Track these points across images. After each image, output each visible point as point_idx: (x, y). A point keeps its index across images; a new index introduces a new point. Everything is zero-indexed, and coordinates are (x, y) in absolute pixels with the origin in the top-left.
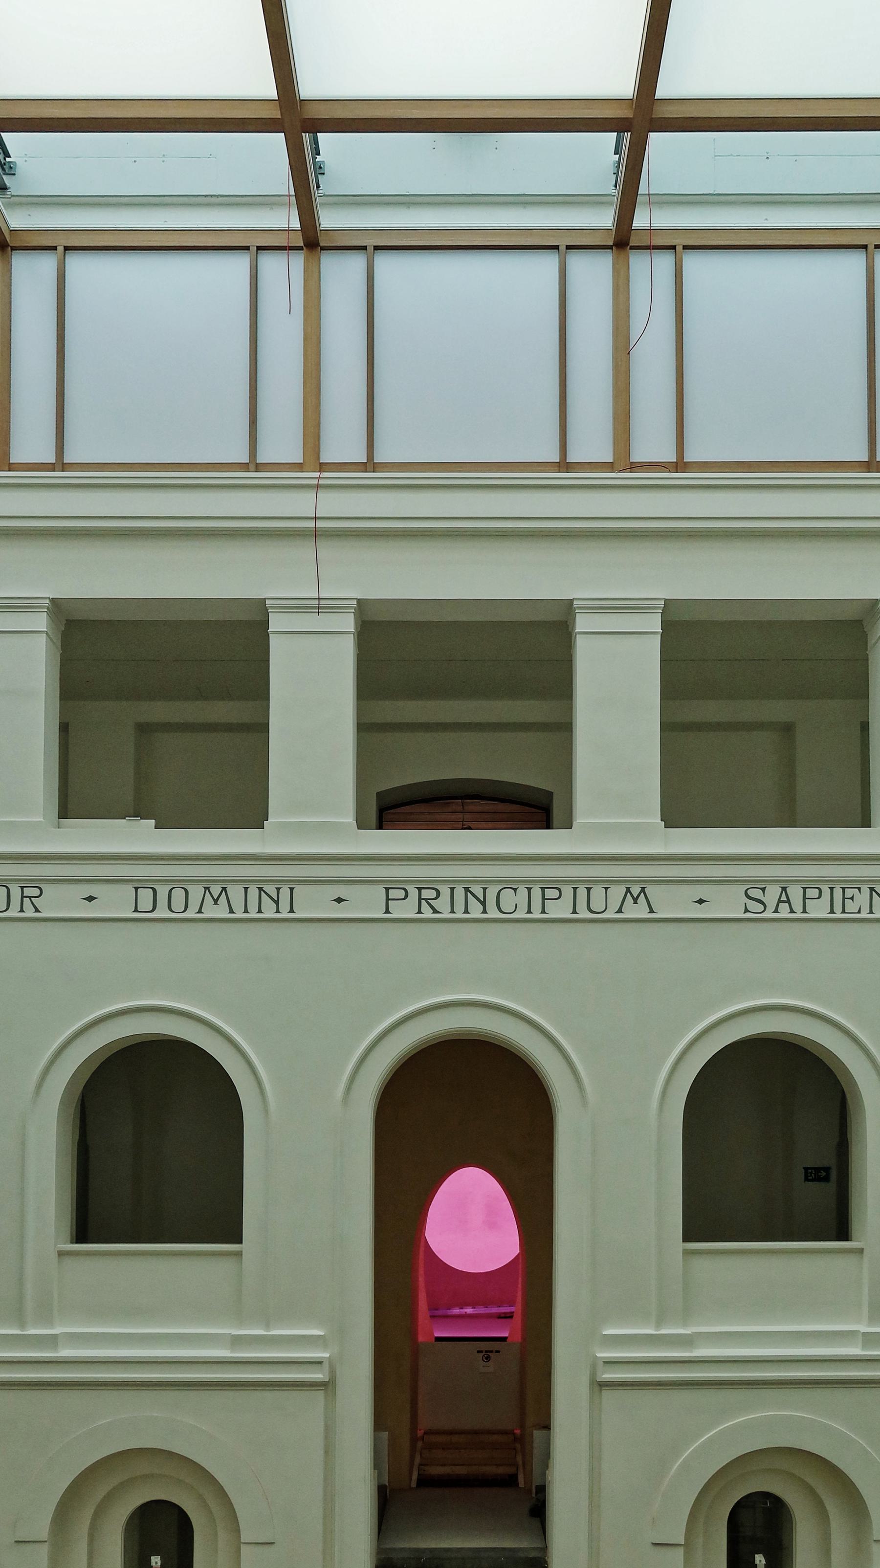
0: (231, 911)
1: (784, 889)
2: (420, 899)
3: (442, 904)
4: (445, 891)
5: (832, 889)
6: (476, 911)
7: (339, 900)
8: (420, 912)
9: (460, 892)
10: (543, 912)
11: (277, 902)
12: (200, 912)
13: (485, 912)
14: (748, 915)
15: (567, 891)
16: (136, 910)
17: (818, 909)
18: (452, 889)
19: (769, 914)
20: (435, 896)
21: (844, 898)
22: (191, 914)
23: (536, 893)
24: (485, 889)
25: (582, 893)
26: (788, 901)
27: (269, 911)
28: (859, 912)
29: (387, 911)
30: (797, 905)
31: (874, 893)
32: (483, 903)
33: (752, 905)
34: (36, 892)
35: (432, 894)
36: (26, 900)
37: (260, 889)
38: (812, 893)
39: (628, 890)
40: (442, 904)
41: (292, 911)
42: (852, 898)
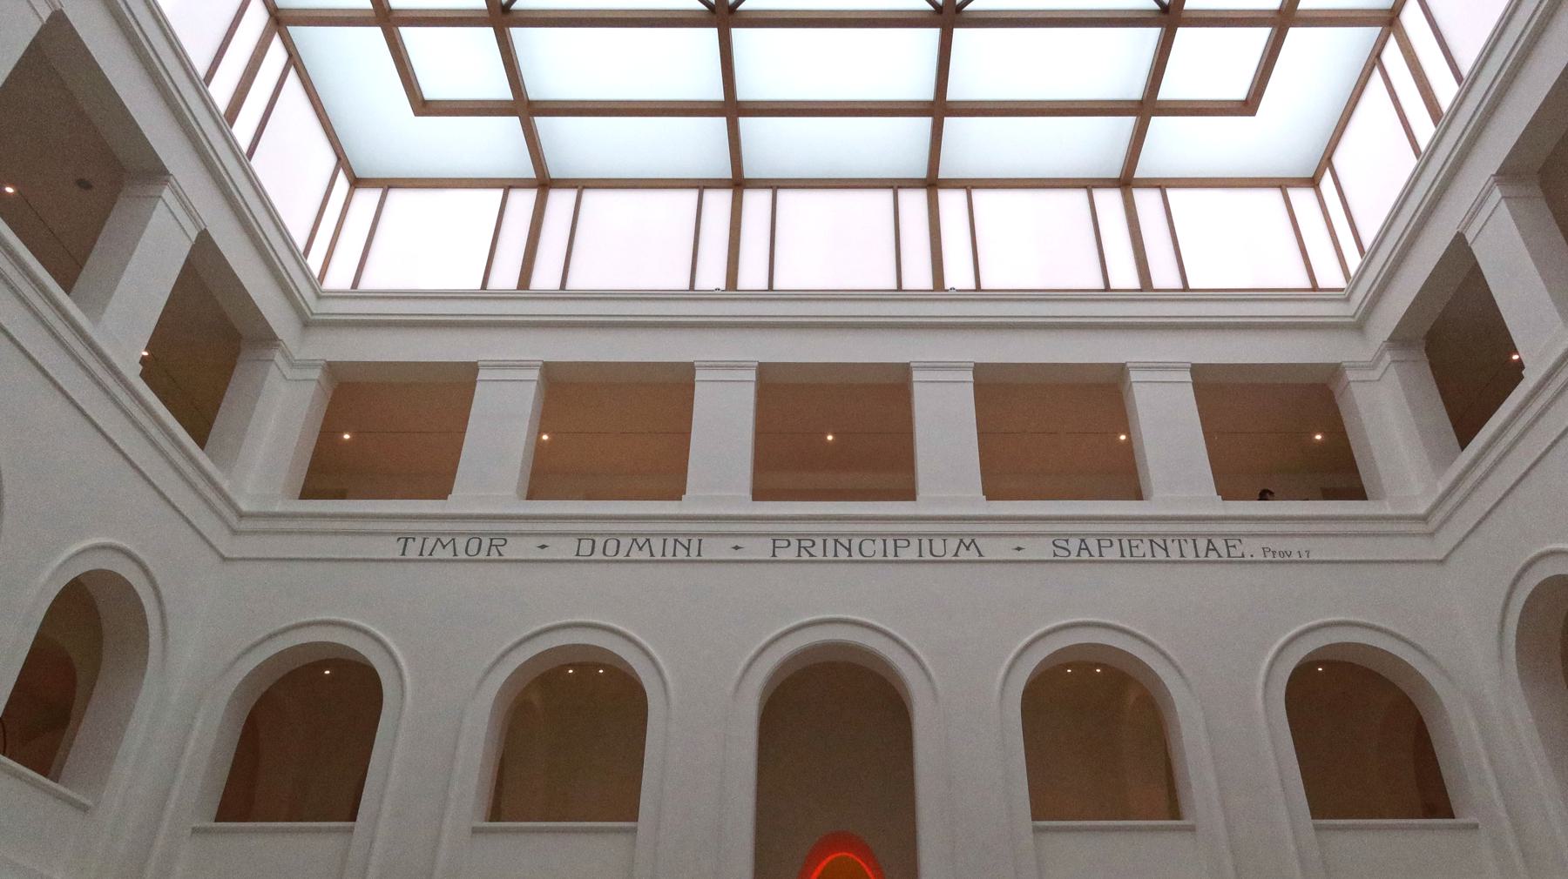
0: (652, 555)
1: (1083, 540)
2: (800, 547)
3: (818, 551)
4: (819, 542)
5: (1120, 540)
6: (843, 554)
7: (737, 548)
8: (799, 556)
9: (830, 543)
10: (896, 555)
11: (688, 549)
12: (628, 555)
13: (850, 555)
14: (1056, 558)
15: (914, 542)
17: (1112, 553)
18: (825, 541)
19: (1073, 557)
20: (811, 545)
21: (1131, 547)
22: (621, 556)
23: (890, 543)
24: (850, 541)
25: (925, 543)
26: (1087, 549)
27: (681, 554)
28: (1144, 556)
29: (774, 555)
30: (1095, 552)
31: (1154, 544)
32: (849, 550)
35: (809, 544)
36: (493, 548)
37: (676, 540)
38: (1105, 543)
39: (961, 541)
40: (818, 551)
41: (699, 555)
42: (1137, 547)
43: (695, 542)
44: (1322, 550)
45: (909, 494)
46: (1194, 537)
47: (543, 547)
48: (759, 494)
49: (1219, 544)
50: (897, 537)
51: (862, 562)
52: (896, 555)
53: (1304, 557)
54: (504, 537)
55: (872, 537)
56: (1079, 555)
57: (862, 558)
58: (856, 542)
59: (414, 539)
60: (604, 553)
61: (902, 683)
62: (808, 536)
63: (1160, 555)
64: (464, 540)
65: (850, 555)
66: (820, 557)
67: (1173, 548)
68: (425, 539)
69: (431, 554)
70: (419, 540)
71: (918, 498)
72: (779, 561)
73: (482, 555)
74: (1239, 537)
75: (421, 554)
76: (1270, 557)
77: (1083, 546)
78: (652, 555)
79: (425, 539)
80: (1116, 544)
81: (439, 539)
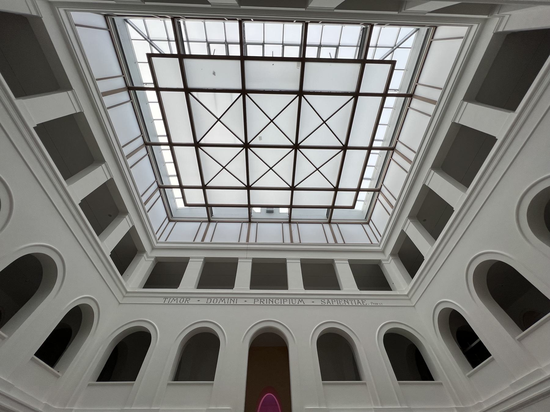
0: (225, 303)
1: (328, 300)
3: (265, 302)
4: (265, 300)
5: (337, 300)
7: (245, 301)
9: (268, 300)
10: (284, 303)
13: (273, 303)
15: (288, 300)
17: (335, 304)
19: (326, 304)
22: (217, 303)
23: (282, 300)
25: (291, 300)
29: (254, 303)
32: (273, 302)
33: (323, 303)
37: (231, 299)
39: (299, 300)
40: (265, 302)
41: (236, 303)
43: (235, 300)
44: (385, 303)
45: (286, 288)
46: (354, 299)
47: (199, 301)
48: (251, 288)
49: (360, 301)
50: (284, 299)
51: (275, 305)
52: (284, 303)
53: (381, 305)
54: (189, 298)
55: (278, 299)
56: (327, 304)
57: (275, 304)
58: (274, 300)
60: (213, 303)
61: (286, 340)
62: (263, 298)
63: (347, 304)
64: (180, 299)
65: (273, 303)
66: (265, 304)
67: (350, 302)
71: (289, 289)
72: (256, 305)
74: (365, 299)
75: (169, 302)
76: (373, 305)
77: (328, 301)
78: (225, 303)
80: (336, 300)
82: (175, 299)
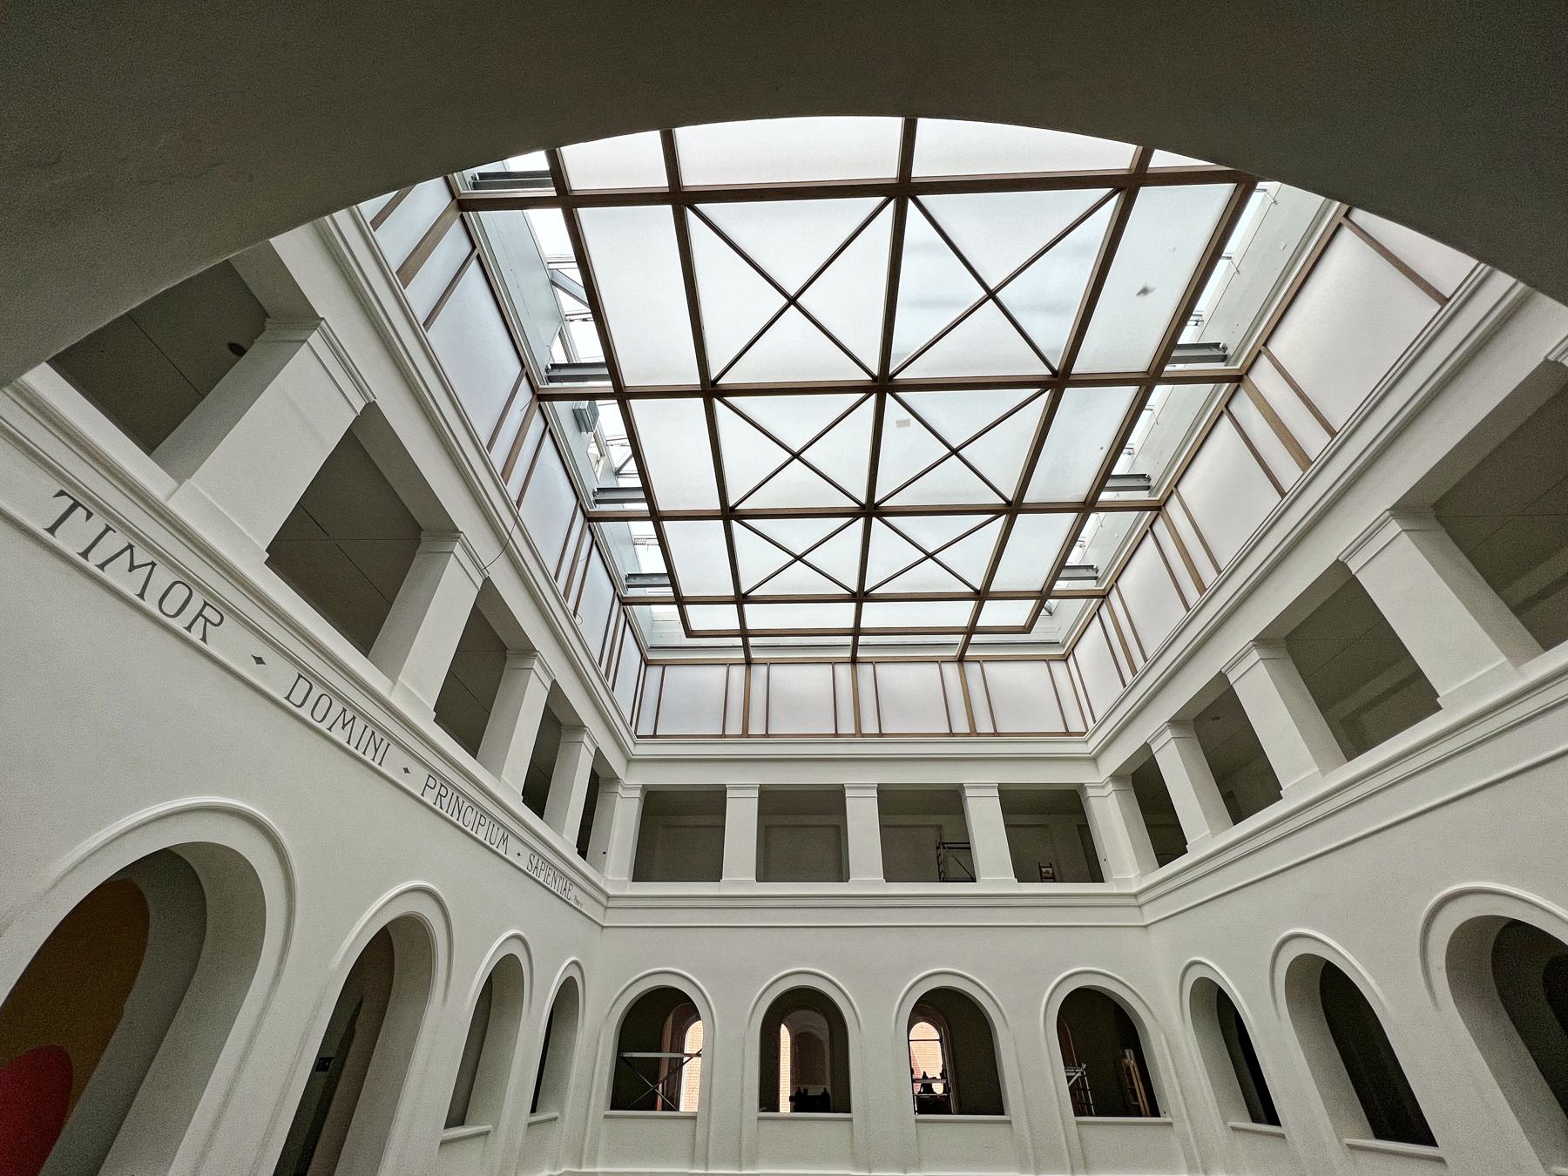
16: (287, 698)
34: (216, 619)
59: (89, 515)
68: (108, 529)
69: (102, 567)
70: (98, 523)
73: (178, 624)
79: (108, 529)
81: (130, 547)
82: (141, 556)
